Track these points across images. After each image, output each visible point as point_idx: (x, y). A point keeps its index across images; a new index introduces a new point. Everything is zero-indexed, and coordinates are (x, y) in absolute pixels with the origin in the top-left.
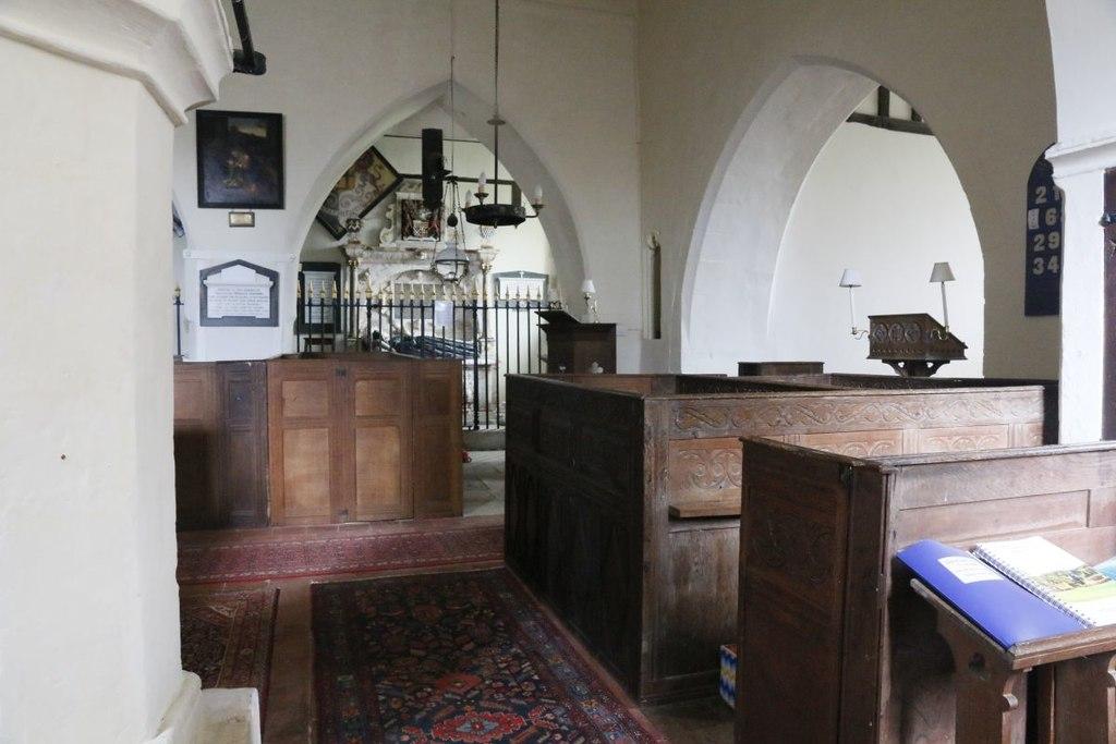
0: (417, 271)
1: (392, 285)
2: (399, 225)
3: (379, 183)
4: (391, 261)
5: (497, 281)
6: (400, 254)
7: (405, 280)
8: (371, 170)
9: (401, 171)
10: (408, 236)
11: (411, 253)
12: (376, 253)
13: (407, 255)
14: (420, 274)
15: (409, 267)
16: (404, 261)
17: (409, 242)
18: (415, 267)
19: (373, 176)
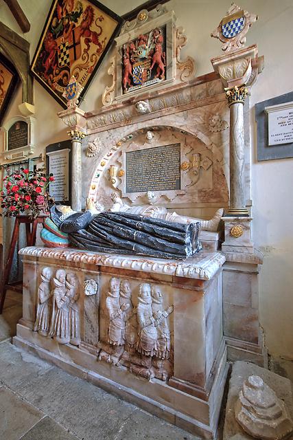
0: (145, 130)
2: (119, 78)
3: (101, 39)
4: (115, 126)
5: (261, 115)
6: (120, 112)
7: (137, 146)
8: (93, 28)
9: (121, 13)
10: (128, 87)
11: (131, 107)
12: (98, 118)
13: (127, 111)
14: (150, 134)
15: (133, 128)
16: (128, 121)
17: (131, 93)
18: (141, 126)
19: (95, 33)
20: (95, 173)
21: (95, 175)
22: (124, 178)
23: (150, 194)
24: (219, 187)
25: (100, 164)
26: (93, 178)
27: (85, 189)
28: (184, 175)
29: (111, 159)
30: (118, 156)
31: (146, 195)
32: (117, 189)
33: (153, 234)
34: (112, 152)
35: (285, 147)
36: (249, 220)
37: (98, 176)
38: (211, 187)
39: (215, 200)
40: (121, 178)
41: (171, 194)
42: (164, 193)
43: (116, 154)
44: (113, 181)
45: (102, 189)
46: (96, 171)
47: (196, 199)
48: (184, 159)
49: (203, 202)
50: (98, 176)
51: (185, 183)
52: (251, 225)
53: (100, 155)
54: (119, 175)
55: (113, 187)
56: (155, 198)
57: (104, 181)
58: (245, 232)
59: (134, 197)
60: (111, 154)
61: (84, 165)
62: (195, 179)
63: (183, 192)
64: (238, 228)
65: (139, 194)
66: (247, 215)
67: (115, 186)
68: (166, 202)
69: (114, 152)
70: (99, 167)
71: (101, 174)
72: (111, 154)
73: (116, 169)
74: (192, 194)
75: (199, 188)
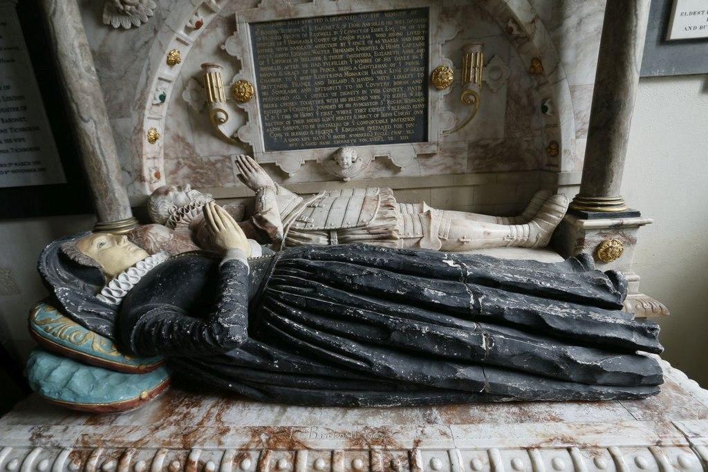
1: (245, 31)
20: (153, 88)
21: (152, 98)
22: (254, 108)
23: (349, 154)
24: (518, 135)
25: (164, 59)
26: (148, 105)
27: (128, 143)
28: (438, 98)
29: (198, 45)
30: (219, 33)
31: (335, 159)
32: (235, 141)
33: (536, 327)
34: (201, 17)
35: (690, 47)
36: (638, 226)
37: (163, 98)
38: (502, 135)
39: (505, 167)
40: (246, 107)
41: (402, 154)
42: (382, 150)
43: (212, 26)
44: (222, 116)
45: (178, 139)
46: (155, 80)
47: (464, 164)
48: (440, 59)
49: (478, 171)
50: (163, 98)
51: (441, 121)
52: (638, 234)
53: (158, 23)
54: (236, 97)
55: (220, 136)
56: (359, 164)
57: (182, 116)
58: (627, 249)
59: (295, 161)
60: (199, 25)
61: (101, 59)
62: (464, 115)
63: (434, 148)
64: (615, 242)
65: (309, 154)
66: (637, 214)
67: (226, 129)
68: (386, 174)
69: (206, 19)
70: (164, 71)
71: (169, 91)
72: (199, 25)
73: (220, 78)
74: (454, 153)
75: (472, 138)
